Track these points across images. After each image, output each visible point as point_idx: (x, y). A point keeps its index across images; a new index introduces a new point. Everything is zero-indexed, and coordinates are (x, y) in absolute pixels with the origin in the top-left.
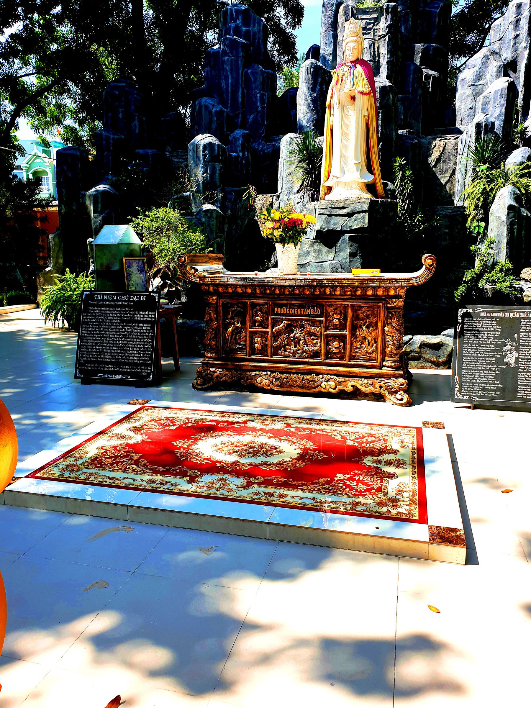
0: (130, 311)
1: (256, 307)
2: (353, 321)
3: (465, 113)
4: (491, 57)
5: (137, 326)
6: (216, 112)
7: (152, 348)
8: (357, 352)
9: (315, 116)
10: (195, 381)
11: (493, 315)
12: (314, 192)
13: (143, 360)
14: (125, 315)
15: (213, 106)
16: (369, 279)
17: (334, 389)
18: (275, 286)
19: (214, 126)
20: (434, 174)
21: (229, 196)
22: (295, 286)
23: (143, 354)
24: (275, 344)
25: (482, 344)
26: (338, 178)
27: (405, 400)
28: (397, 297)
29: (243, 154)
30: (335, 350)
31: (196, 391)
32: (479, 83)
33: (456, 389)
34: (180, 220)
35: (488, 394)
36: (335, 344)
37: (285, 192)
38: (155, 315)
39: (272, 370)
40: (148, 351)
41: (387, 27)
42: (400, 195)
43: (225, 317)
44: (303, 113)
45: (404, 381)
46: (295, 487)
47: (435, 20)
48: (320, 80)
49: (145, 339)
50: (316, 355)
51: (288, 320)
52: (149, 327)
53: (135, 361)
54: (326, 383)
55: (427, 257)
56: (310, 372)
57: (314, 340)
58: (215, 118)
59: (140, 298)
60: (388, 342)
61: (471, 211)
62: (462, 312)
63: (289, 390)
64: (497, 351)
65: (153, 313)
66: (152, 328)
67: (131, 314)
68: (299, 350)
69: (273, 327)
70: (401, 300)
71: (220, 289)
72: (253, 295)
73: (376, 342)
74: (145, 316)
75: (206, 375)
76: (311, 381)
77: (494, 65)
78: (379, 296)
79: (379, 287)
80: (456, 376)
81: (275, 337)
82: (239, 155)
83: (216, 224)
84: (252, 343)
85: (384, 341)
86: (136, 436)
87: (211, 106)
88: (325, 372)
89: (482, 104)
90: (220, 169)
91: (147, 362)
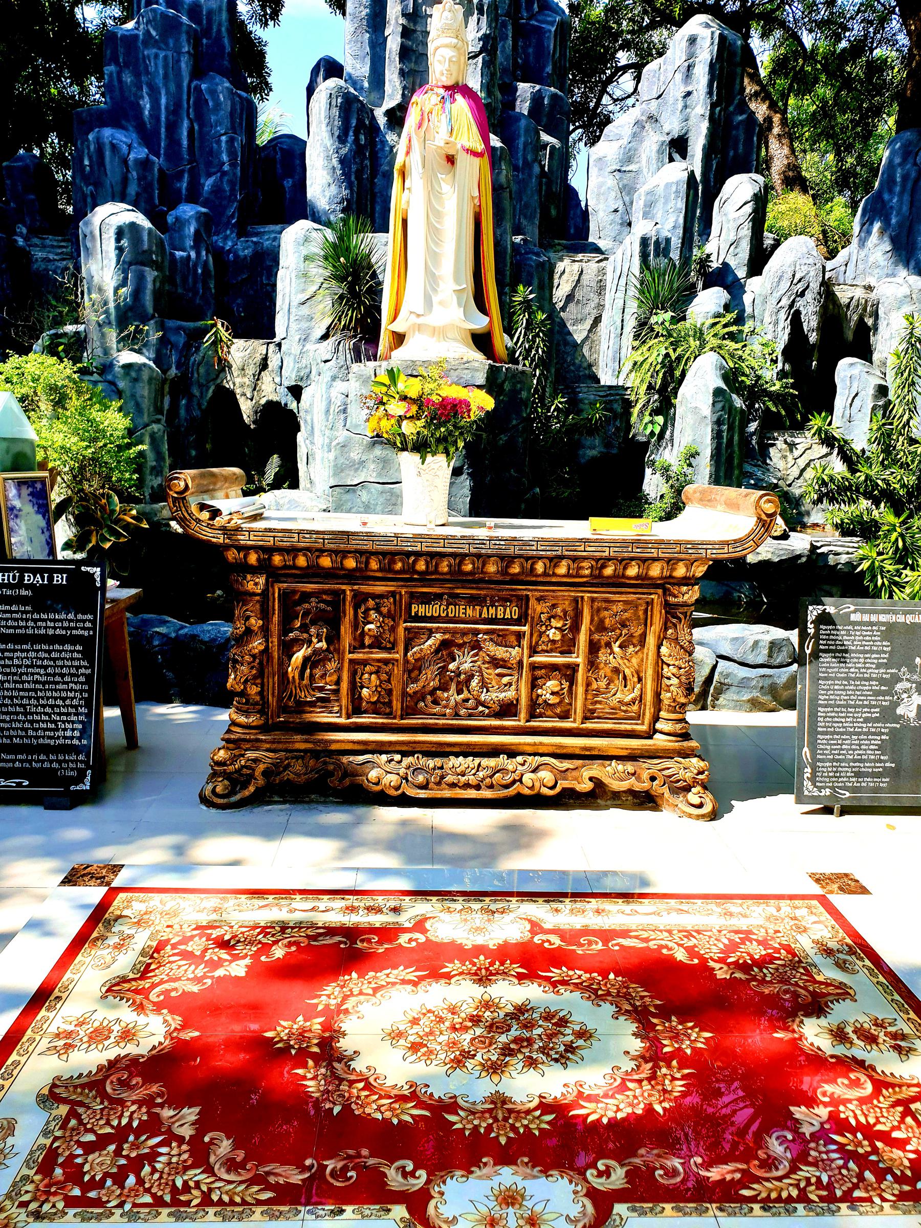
0: (23, 612)
1: (365, 601)
2: (591, 633)
3: (606, 218)
4: (647, 126)
5: (46, 651)
6: (136, 160)
7: (88, 705)
8: (600, 702)
9: (345, 192)
10: (210, 787)
11: (874, 618)
12: (361, 340)
13: (65, 738)
14: (10, 623)
15: (130, 146)
16: (635, 542)
17: (552, 788)
18: (418, 554)
19: (133, 189)
20: (563, 324)
21: (173, 338)
22: (466, 555)
23: (64, 722)
24: (412, 688)
25: (854, 679)
26: (418, 316)
27: (708, 808)
28: (687, 581)
29: (198, 254)
30: (553, 700)
31: (213, 811)
32: (627, 169)
33: (806, 776)
34: (75, 383)
35: (867, 782)
36: (552, 685)
37: (295, 337)
38: (93, 622)
39: (404, 748)
40: (76, 714)
41: (480, 40)
42: (525, 359)
43: (286, 627)
44: (322, 183)
45: (702, 764)
46: (331, 931)
47: (548, 46)
48: (354, 122)
49: (67, 683)
50: (507, 709)
51: (445, 631)
52: (78, 652)
53: (41, 741)
54: (532, 775)
55: (761, 497)
56: (494, 752)
57: (502, 675)
58: (134, 173)
59: (51, 579)
60: (669, 678)
61: (640, 396)
62: (815, 613)
63: (447, 793)
64: (883, 693)
65: (90, 617)
66: (87, 654)
67: (27, 620)
68: (467, 700)
69: (406, 651)
70: (697, 587)
71: (277, 559)
72: (360, 575)
73: (640, 680)
74: (66, 624)
75: (238, 771)
76: (498, 771)
77: (653, 141)
78: (652, 578)
79: (655, 560)
80: (806, 749)
81: (410, 672)
82: (189, 256)
83: (150, 392)
84: (354, 688)
85: (659, 677)
86: (142, 1020)
87: (125, 148)
88: (529, 749)
89: (645, 206)
90: (154, 281)
91: (76, 742)
